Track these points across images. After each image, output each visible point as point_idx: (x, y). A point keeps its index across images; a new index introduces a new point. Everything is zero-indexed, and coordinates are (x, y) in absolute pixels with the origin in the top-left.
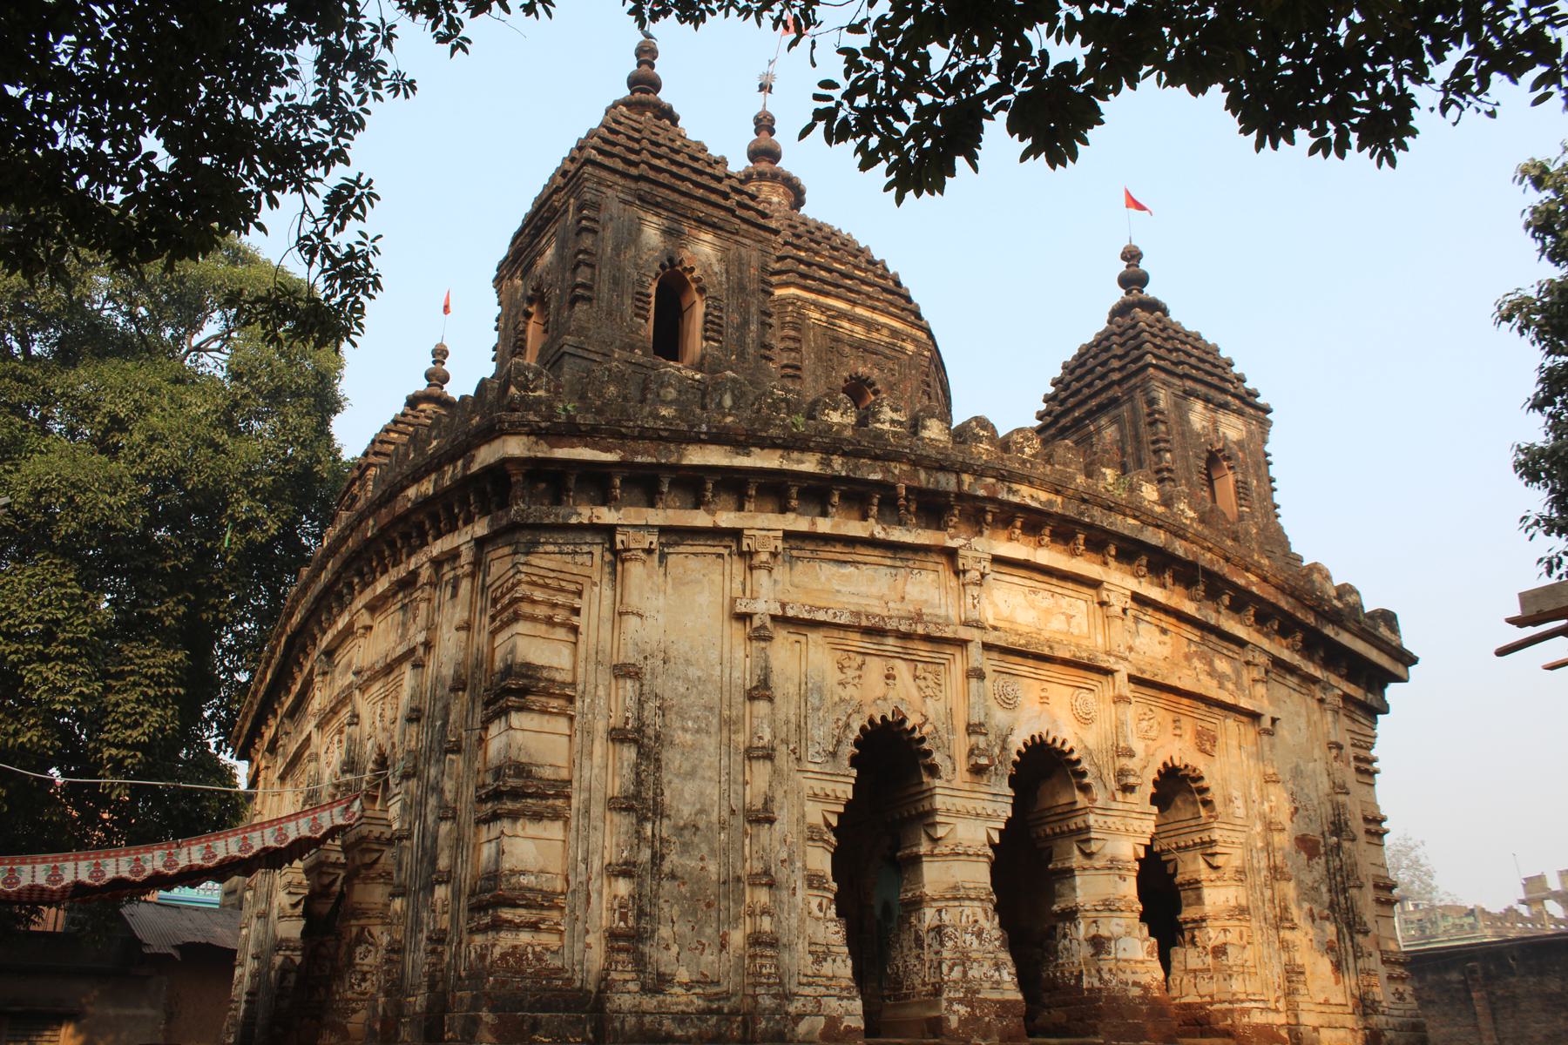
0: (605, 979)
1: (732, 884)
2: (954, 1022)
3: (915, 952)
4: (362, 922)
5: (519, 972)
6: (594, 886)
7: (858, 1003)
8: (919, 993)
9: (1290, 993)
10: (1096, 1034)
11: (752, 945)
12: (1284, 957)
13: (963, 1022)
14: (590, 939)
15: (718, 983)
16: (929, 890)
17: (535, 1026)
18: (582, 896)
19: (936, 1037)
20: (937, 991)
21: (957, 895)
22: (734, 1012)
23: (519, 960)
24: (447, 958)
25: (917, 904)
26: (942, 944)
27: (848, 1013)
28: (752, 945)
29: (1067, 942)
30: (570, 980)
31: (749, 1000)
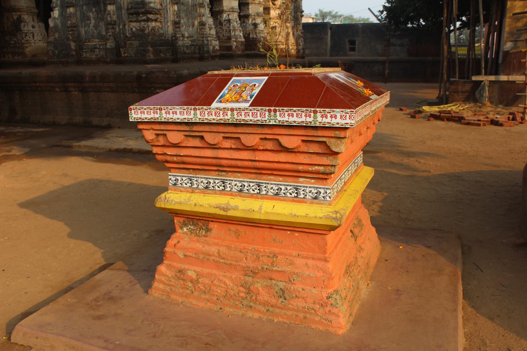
0: (175, 36)
1: (194, 6)
2: (234, 48)
3: (219, 27)
4: (19, 13)
5: (155, 35)
6: (168, 7)
7: (218, 42)
8: (222, 39)
9: (287, 40)
10: (254, 50)
11: (200, 26)
12: (286, 30)
13: (236, 47)
14: (169, 24)
15: (192, 37)
16: (225, 8)
17: (160, 52)
18: (165, 10)
19: (229, 51)
20: (229, 38)
21: (232, 10)
22: (196, 45)
23: (155, 31)
24: (117, 30)
25: (222, 12)
26: (230, 25)
27: (216, 45)
28: (200, 26)
29: (245, 24)
30: (165, 37)
31: (201, 42)
